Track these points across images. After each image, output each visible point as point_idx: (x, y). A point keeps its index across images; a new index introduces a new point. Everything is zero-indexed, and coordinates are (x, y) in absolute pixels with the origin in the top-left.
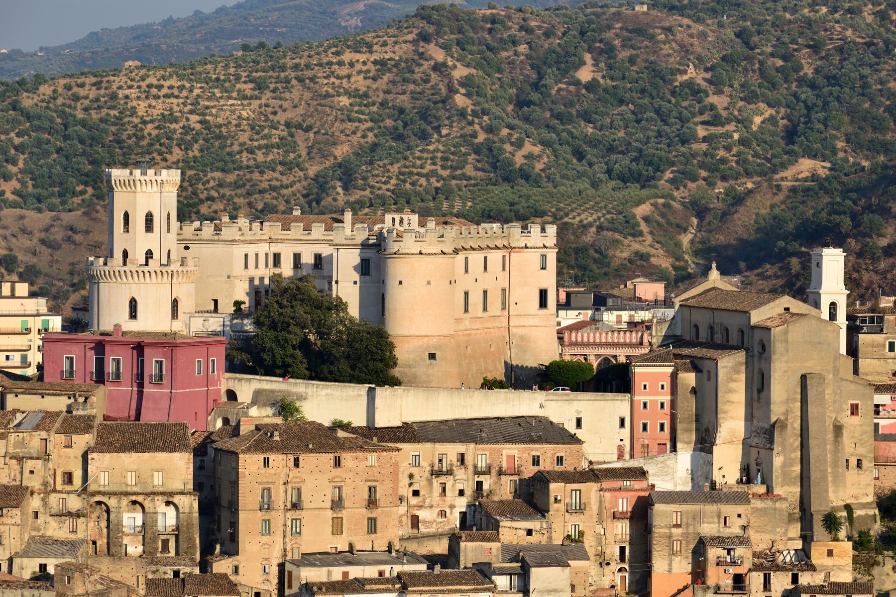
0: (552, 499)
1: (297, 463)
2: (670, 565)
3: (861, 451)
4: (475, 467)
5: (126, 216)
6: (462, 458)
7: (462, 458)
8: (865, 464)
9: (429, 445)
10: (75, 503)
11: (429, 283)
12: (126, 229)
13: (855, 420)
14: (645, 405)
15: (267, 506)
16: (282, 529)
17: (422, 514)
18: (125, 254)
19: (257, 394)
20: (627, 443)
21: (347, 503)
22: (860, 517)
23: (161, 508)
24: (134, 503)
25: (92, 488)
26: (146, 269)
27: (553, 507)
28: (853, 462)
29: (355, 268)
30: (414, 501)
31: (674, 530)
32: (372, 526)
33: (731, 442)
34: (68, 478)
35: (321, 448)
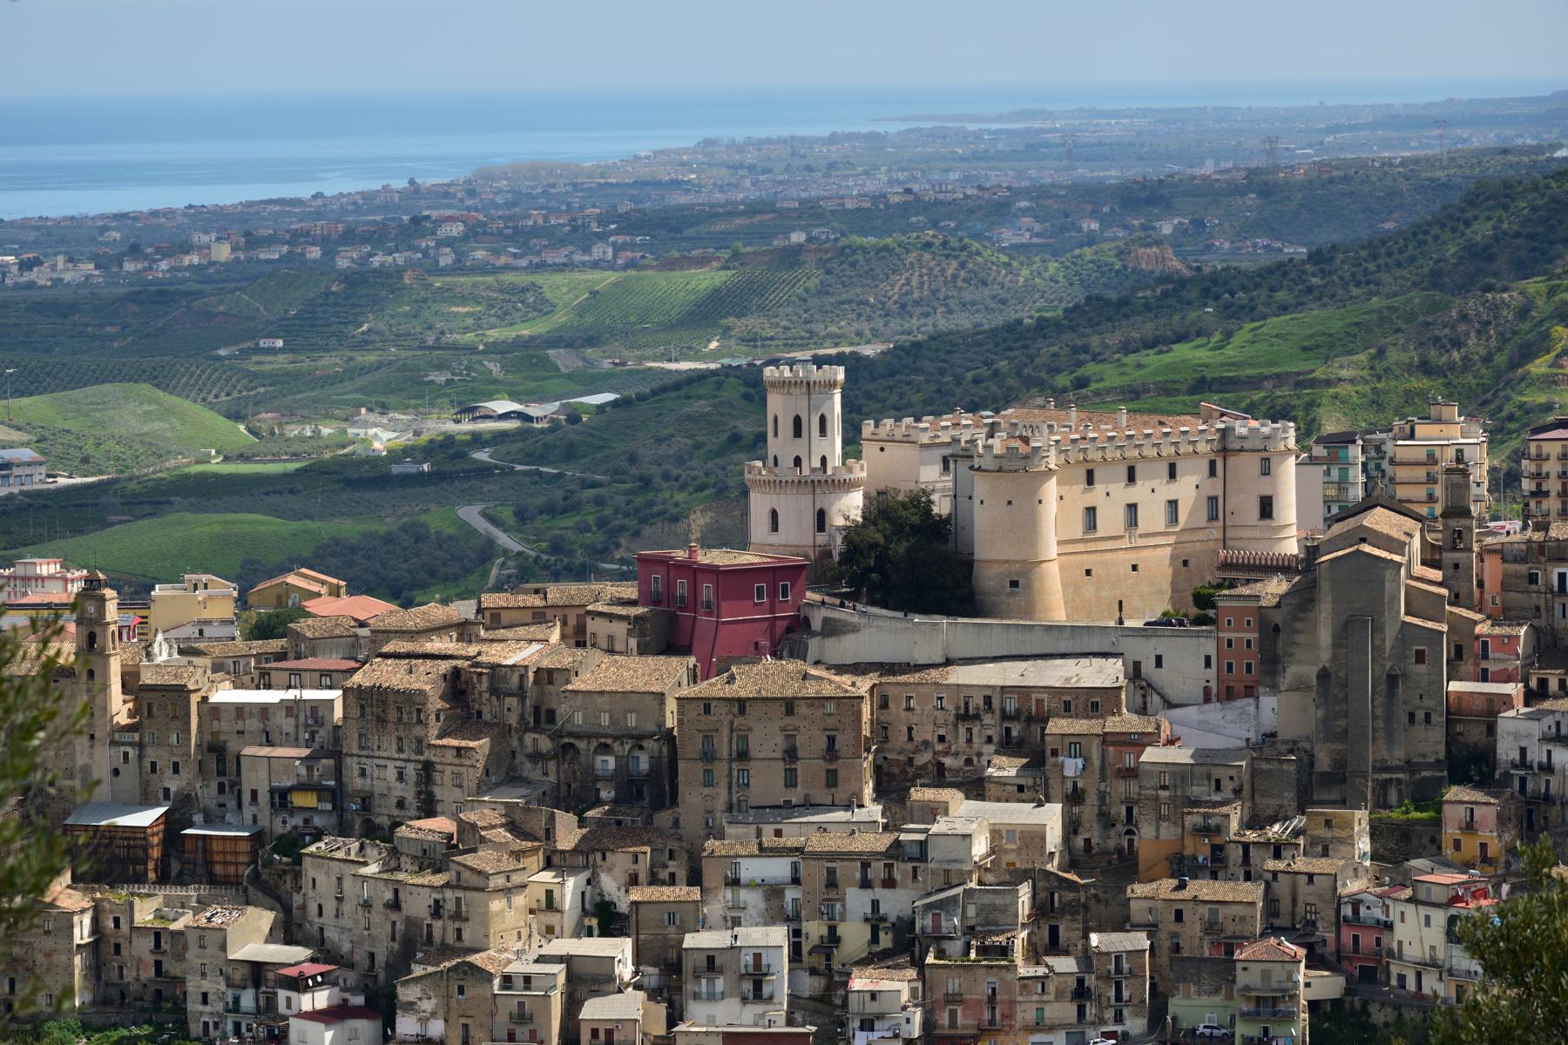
0: (1048, 753)
2: (1158, 830)
4: (1003, 710)
8: (1434, 718)
10: (545, 744)
11: (1010, 503)
12: (776, 435)
14: (1230, 645)
15: (708, 756)
16: (726, 780)
17: (948, 761)
18: (776, 464)
19: (826, 620)
20: (1213, 685)
21: (800, 754)
23: (637, 753)
24: (606, 745)
25: (568, 727)
28: (1420, 715)
30: (939, 747)
31: (1164, 794)
33: (1298, 689)
34: (551, 715)
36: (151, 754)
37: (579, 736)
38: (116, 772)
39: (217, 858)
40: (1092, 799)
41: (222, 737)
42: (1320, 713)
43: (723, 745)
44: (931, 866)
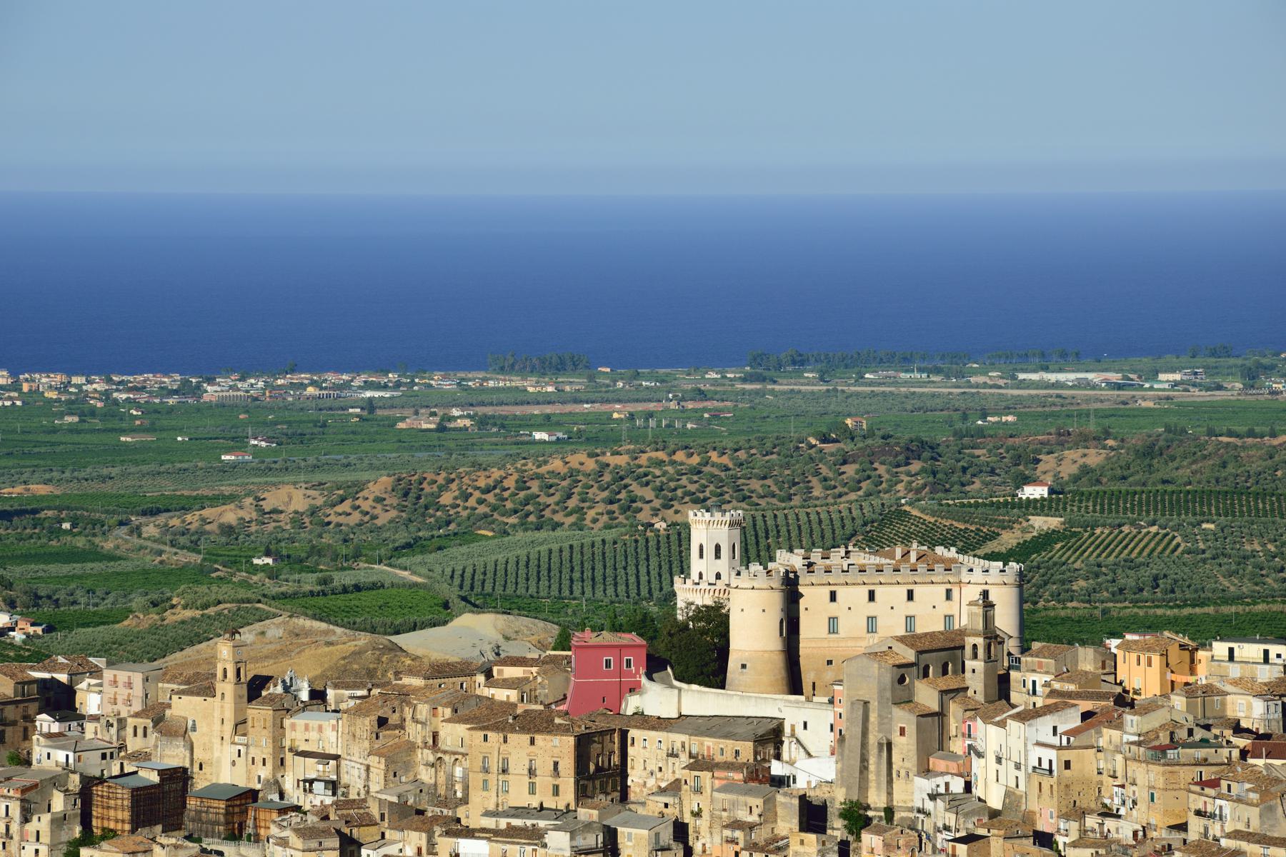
1: (505, 741)
3: (907, 764)
5: (701, 546)
6: (683, 746)
7: (683, 746)
9: (665, 734)
13: (903, 739)
21: (538, 772)
22: (902, 818)
26: (713, 588)
27: (685, 787)
28: (903, 773)
29: (802, 596)
30: (659, 775)
32: (556, 791)
35: (524, 730)
36: (252, 750)
37: (445, 752)
38: (234, 763)
39: (262, 824)
40: (705, 814)
41: (297, 743)
42: (839, 765)
43: (494, 766)
44: (550, 852)
